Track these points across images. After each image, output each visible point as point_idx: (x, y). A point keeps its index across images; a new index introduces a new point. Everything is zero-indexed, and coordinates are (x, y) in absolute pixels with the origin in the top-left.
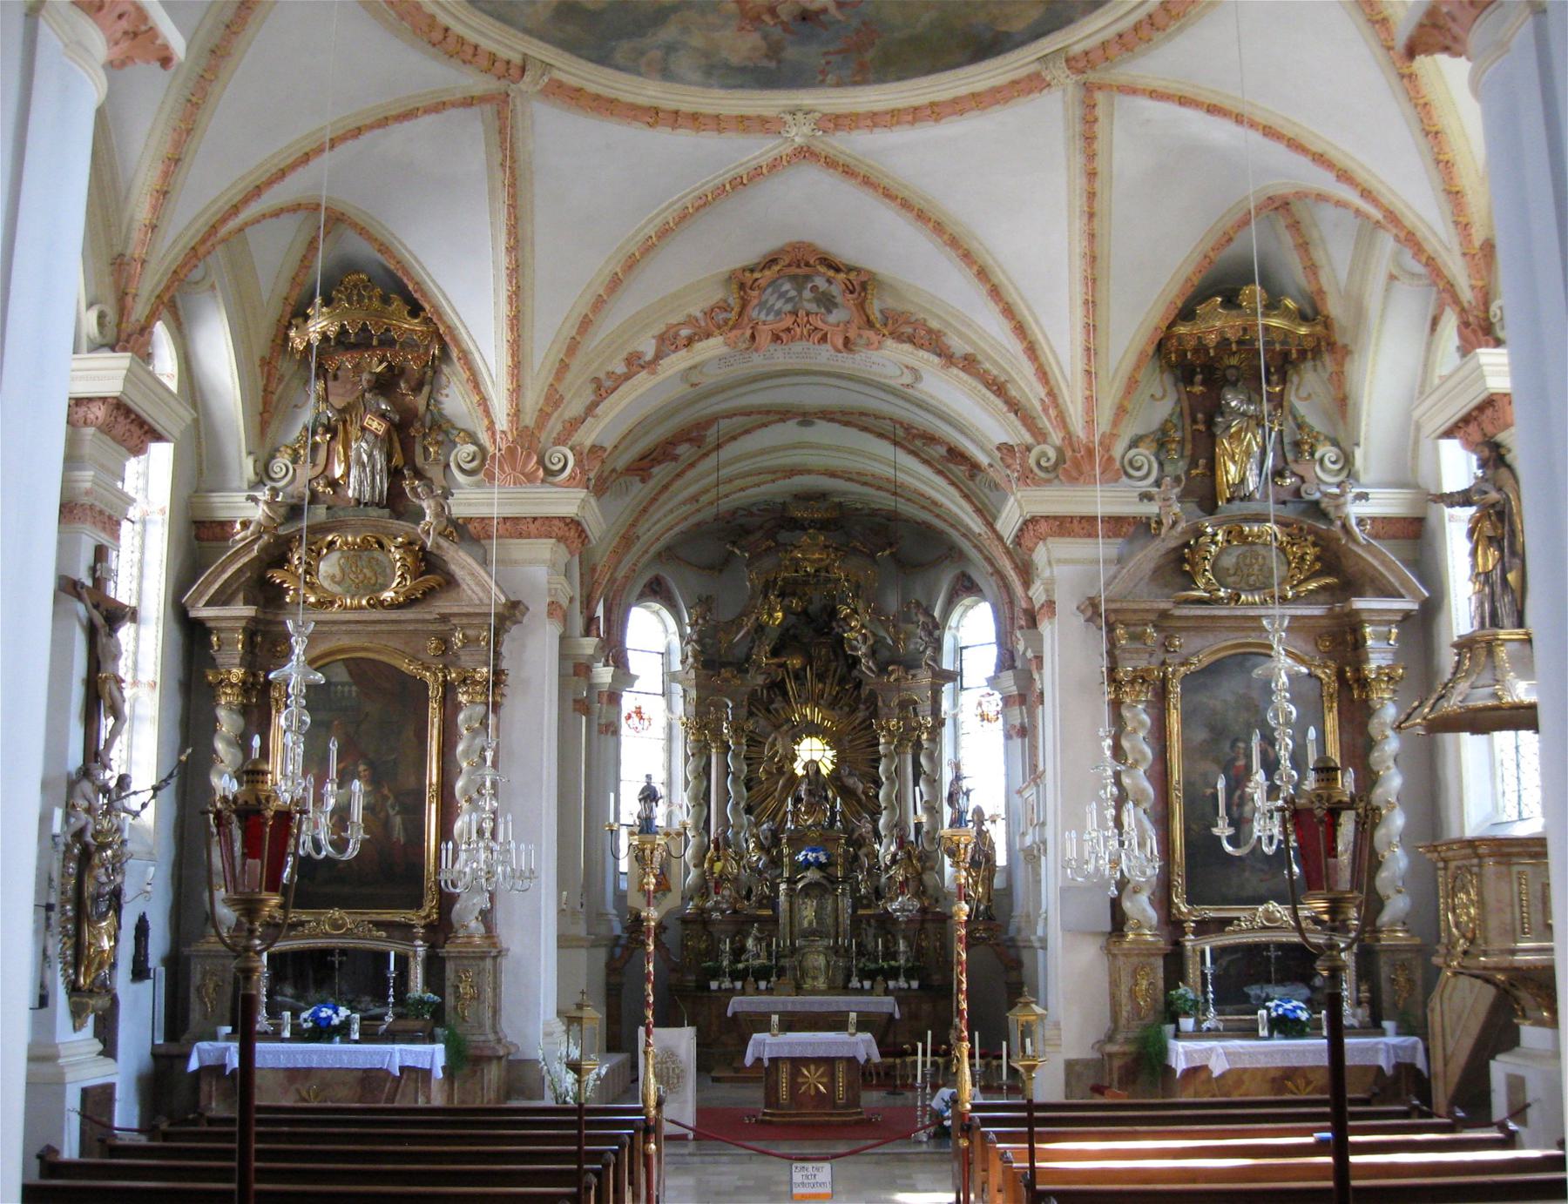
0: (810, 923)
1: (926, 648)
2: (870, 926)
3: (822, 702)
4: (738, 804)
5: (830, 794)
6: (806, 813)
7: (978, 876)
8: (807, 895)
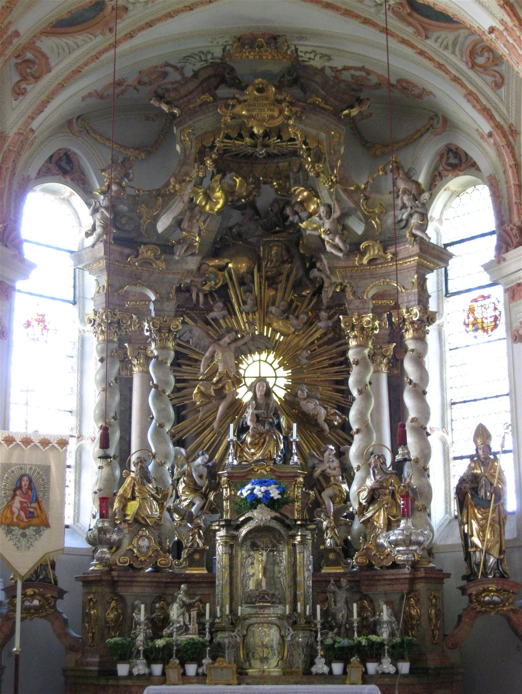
0: (258, 584)
1: (411, 215)
2: (340, 587)
3: (273, 309)
4: (161, 426)
5: (284, 424)
6: (253, 444)
7: (486, 518)
8: (254, 547)
